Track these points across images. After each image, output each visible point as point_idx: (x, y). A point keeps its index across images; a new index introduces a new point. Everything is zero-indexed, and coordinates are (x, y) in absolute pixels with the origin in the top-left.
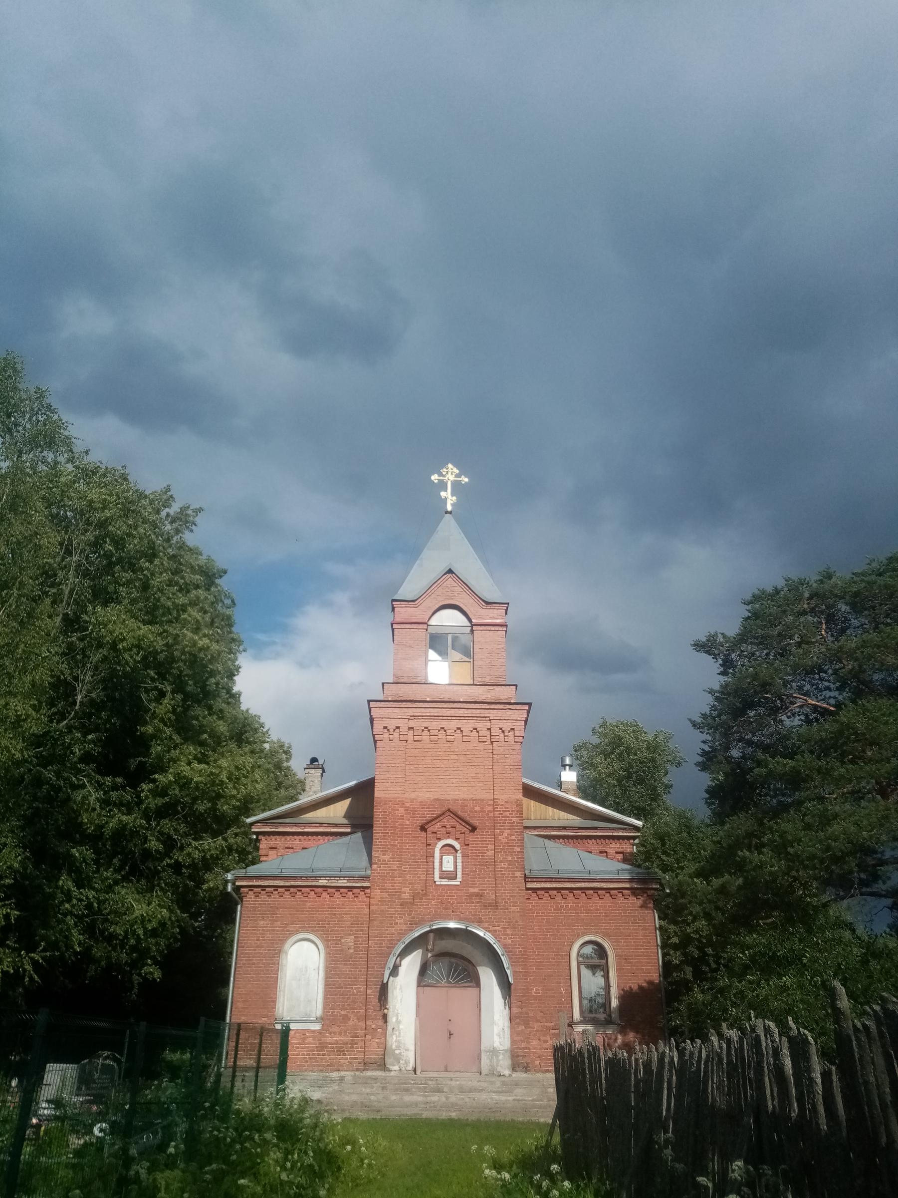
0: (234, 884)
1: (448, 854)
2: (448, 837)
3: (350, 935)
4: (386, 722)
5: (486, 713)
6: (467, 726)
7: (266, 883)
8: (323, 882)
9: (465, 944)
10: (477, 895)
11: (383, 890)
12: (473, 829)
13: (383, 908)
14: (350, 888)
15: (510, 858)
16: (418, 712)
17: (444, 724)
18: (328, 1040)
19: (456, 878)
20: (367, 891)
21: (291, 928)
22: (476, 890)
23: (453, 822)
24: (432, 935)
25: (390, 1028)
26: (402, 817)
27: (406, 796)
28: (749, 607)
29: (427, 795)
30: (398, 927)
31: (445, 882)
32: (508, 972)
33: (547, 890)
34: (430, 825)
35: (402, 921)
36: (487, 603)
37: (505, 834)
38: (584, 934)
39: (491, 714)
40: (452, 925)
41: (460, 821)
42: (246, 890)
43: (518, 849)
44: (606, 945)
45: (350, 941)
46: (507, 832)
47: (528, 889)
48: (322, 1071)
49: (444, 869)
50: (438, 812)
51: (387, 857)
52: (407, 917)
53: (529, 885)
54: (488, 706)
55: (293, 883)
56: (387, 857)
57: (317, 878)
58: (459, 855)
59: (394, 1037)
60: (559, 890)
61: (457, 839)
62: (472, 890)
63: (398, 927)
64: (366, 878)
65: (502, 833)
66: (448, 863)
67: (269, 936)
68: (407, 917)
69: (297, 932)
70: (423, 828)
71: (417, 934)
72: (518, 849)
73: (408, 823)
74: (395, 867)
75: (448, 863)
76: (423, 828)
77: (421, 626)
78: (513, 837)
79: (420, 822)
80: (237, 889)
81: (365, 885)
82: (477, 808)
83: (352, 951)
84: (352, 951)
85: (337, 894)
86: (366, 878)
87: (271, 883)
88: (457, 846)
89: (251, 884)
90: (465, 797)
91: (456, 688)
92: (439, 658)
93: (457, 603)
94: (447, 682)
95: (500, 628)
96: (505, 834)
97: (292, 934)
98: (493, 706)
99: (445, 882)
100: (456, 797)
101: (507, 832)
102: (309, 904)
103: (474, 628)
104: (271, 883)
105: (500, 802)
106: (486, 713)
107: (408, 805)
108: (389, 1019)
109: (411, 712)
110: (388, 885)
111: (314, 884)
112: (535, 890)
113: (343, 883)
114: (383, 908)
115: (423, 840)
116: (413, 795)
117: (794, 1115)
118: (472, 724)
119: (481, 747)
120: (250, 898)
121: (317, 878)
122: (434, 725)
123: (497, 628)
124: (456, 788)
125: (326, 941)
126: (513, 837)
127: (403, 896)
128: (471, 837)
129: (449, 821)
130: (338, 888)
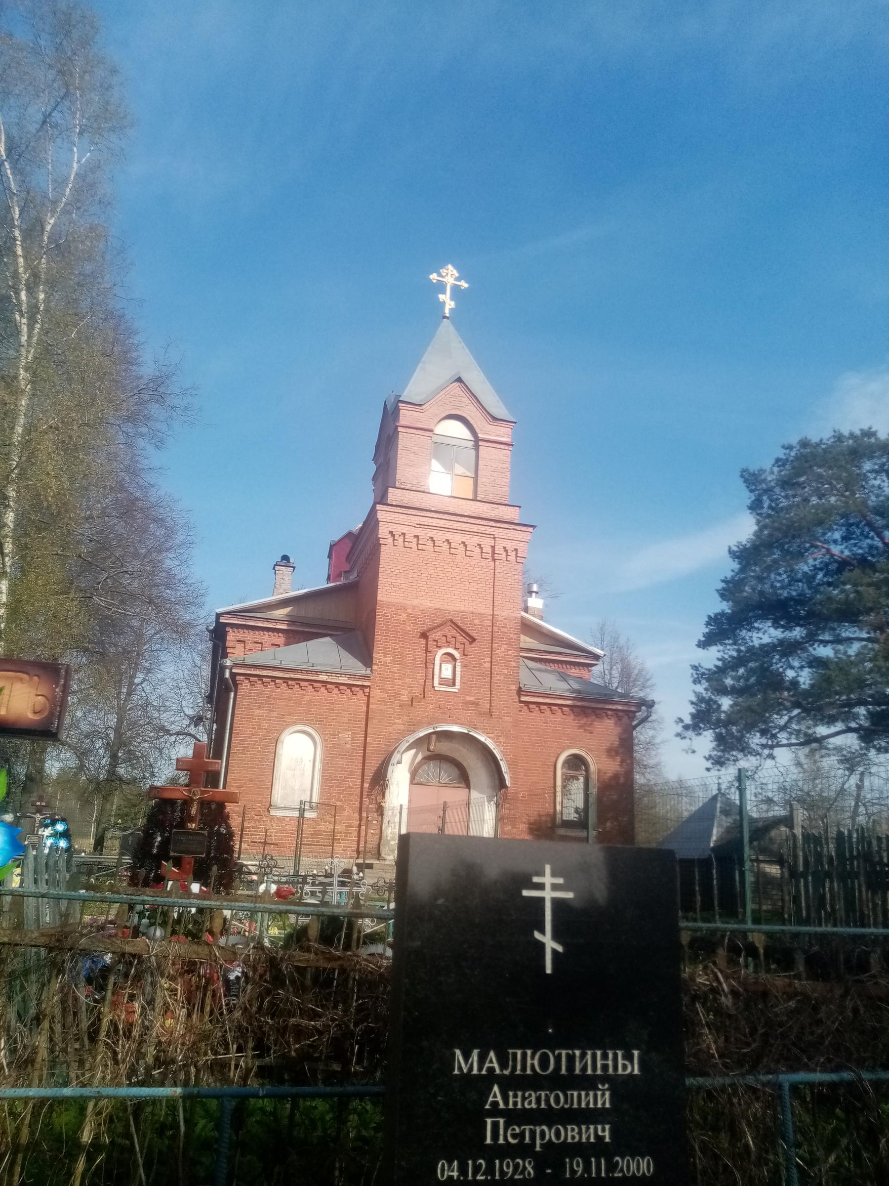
0: (231, 669)
1: (447, 662)
2: (448, 646)
3: (348, 730)
4: (392, 527)
5: (491, 530)
6: (472, 541)
7: (265, 673)
8: (323, 677)
9: (461, 748)
10: (473, 703)
11: (382, 690)
12: (473, 640)
13: (382, 707)
14: (350, 686)
15: (506, 672)
16: (424, 521)
17: (449, 536)
18: (323, 828)
19: (454, 685)
20: (367, 690)
21: (288, 719)
22: (472, 699)
23: (454, 632)
24: (434, 737)
25: (385, 821)
26: (404, 623)
27: (408, 602)
28: (785, 451)
29: (428, 603)
30: (396, 727)
31: (443, 688)
32: (506, 776)
33: (538, 704)
34: (431, 632)
35: (400, 721)
36: (495, 419)
37: (503, 649)
38: (569, 747)
39: (497, 532)
40: (455, 728)
41: (462, 633)
42: (242, 678)
43: (514, 664)
44: (589, 759)
45: (347, 736)
46: (504, 647)
47: (521, 702)
48: (316, 857)
49: (442, 676)
50: (439, 621)
51: (387, 659)
52: (406, 718)
53: (523, 699)
54: (494, 524)
55: (292, 676)
56: (387, 659)
57: (317, 673)
58: (458, 664)
59: (390, 829)
60: (549, 705)
61: (456, 649)
62: (468, 698)
63: (396, 727)
64: (366, 677)
65: (499, 648)
66: (447, 671)
67: (264, 725)
68: (406, 718)
69: (295, 723)
70: (424, 635)
71: (421, 734)
72: (514, 664)
73: (409, 628)
74: (395, 670)
75: (447, 671)
76: (424, 635)
77: (427, 433)
78: (510, 653)
79: (421, 629)
80: (233, 675)
81: (365, 684)
82: (477, 622)
83: (349, 746)
84: (349, 746)
85: (336, 691)
86: (366, 677)
87: (270, 673)
88: (457, 655)
89: (248, 672)
90: (465, 609)
91: (452, 500)
92: (442, 470)
93: (464, 415)
94: (449, 494)
95: (506, 447)
96: (503, 649)
97: (288, 725)
98: (498, 525)
99: (443, 688)
100: (457, 609)
101: (504, 647)
102: (307, 698)
103: (481, 443)
104: (270, 673)
105: (499, 618)
106: (491, 530)
107: (409, 611)
108: (386, 813)
109: (418, 520)
110: (388, 686)
111: (314, 678)
112: (527, 703)
113: (343, 680)
114: (382, 707)
115: (423, 646)
116: (416, 602)
117: (804, 915)
118: (476, 540)
119: (483, 563)
120: (245, 686)
121: (317, 673)
122: (439, 536)
123: (503, 447)
124: (461, 600)
125: (323, 735)
126: (510, 653)
127: (402, 698)
128: (470, 648)
129: (451, 632)
130: (337, 685)
